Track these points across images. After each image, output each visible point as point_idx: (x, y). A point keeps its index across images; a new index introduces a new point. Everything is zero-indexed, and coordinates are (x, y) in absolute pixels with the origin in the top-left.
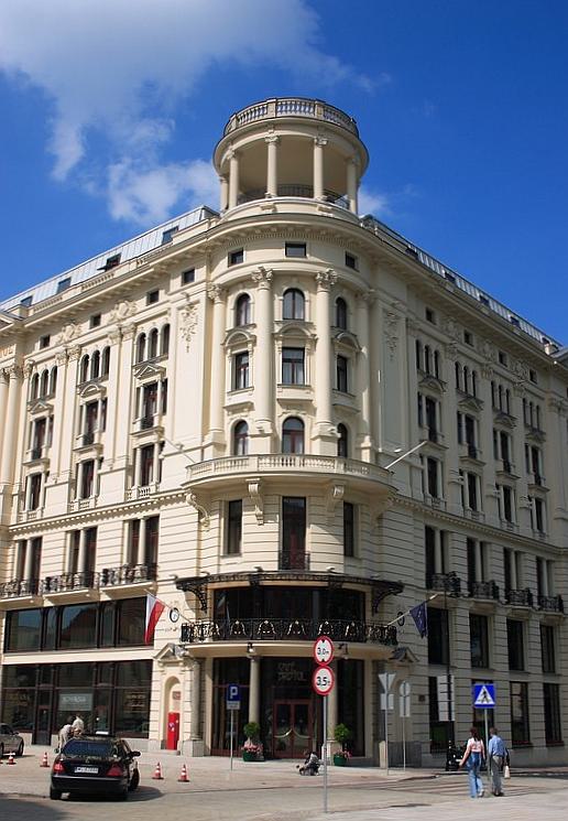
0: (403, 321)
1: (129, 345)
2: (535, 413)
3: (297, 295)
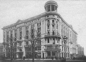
1: (36, 24)
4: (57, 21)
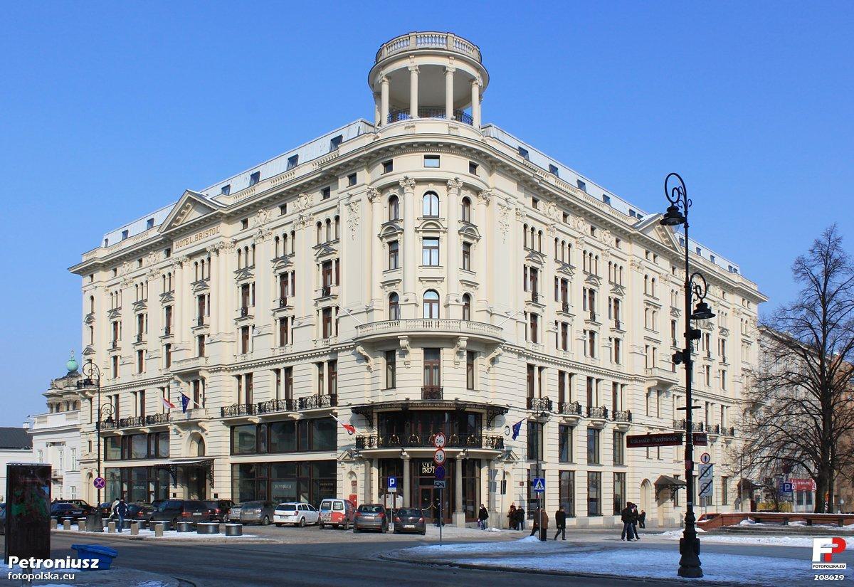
0: (514, 211)
2: (618, 273)
3: (432, 195)
4: (467, 201)
